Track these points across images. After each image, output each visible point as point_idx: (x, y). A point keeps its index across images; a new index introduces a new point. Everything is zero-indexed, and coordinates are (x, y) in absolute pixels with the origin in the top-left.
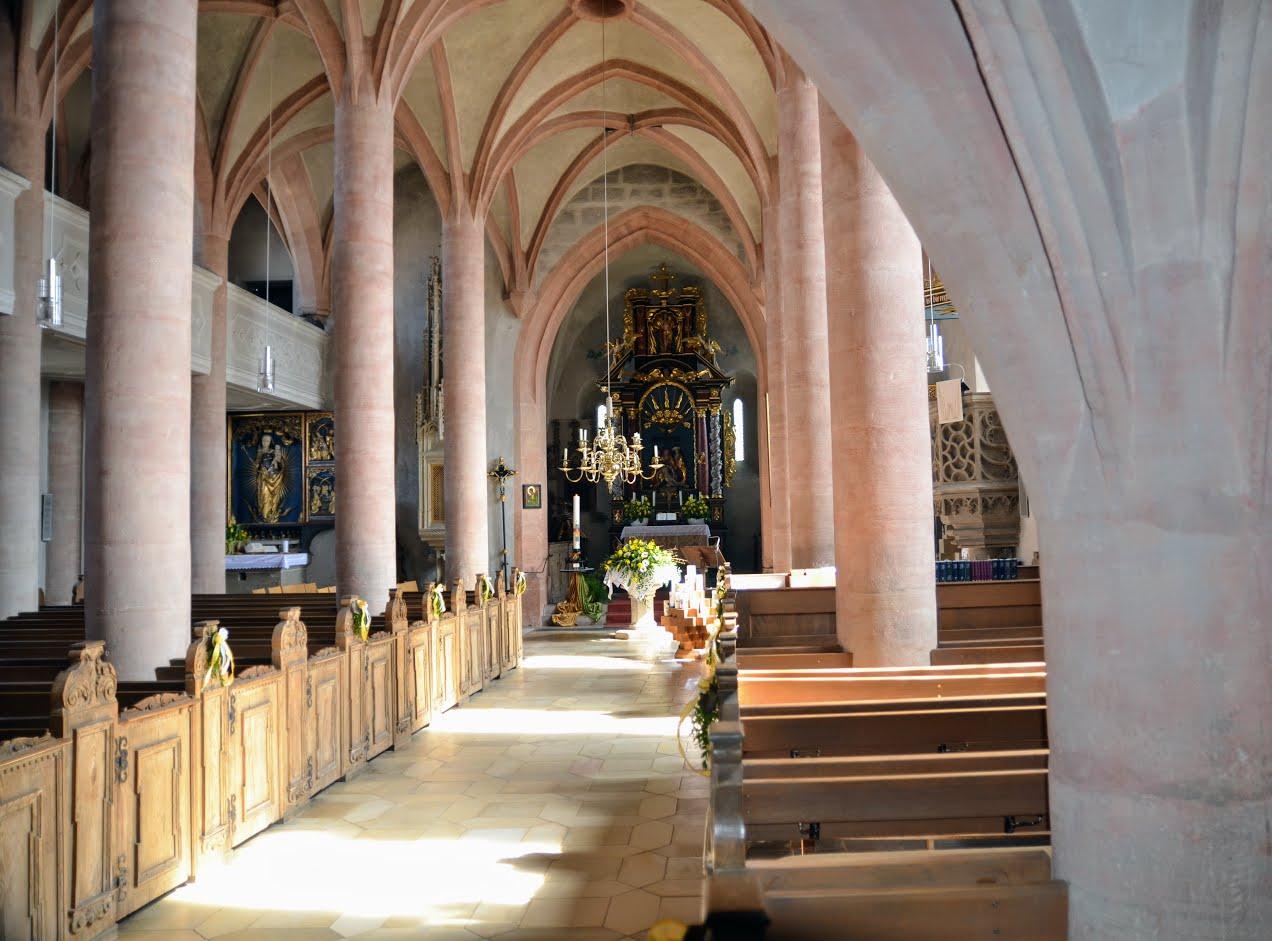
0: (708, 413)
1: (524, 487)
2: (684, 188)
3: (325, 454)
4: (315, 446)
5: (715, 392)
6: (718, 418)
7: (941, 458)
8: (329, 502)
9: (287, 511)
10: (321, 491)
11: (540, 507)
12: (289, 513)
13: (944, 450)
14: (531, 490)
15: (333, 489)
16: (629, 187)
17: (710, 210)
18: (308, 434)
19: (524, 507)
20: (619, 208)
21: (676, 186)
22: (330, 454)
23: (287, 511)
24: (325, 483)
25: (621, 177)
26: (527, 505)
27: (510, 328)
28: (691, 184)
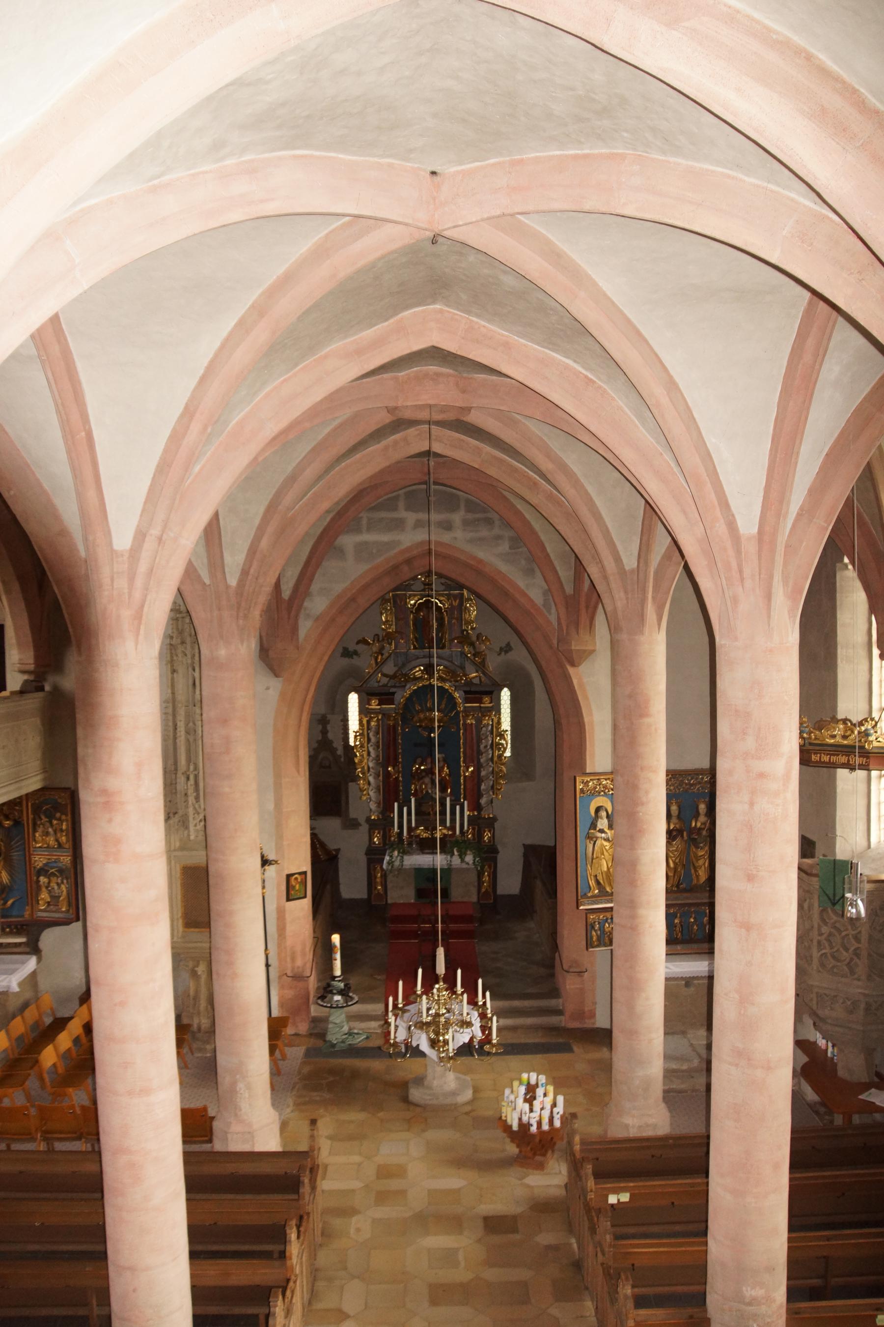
0: (479, 721)
1: (289, 876)
2: (478, 520)
3: (51, 840)
4: (40, 830)
5: (486, 699)
6: (490, 727)
7: (815, 943)
8: (60, 897)
9: (10, 902)
10: (49, 883)
11: (305, 897)
12: (13, 904)
13: (821, 934)
14: (296, 879)
15: (62, 882)
16: (411, 517)
17: (510, 548)
18: (31, 816)
19: (288, 899)
21: (470, 516)
22: (57, 840)
23: (10, 902)
24: (53, 874)
25: (401, 504)
26: (291, 898)
27: (268, 688)
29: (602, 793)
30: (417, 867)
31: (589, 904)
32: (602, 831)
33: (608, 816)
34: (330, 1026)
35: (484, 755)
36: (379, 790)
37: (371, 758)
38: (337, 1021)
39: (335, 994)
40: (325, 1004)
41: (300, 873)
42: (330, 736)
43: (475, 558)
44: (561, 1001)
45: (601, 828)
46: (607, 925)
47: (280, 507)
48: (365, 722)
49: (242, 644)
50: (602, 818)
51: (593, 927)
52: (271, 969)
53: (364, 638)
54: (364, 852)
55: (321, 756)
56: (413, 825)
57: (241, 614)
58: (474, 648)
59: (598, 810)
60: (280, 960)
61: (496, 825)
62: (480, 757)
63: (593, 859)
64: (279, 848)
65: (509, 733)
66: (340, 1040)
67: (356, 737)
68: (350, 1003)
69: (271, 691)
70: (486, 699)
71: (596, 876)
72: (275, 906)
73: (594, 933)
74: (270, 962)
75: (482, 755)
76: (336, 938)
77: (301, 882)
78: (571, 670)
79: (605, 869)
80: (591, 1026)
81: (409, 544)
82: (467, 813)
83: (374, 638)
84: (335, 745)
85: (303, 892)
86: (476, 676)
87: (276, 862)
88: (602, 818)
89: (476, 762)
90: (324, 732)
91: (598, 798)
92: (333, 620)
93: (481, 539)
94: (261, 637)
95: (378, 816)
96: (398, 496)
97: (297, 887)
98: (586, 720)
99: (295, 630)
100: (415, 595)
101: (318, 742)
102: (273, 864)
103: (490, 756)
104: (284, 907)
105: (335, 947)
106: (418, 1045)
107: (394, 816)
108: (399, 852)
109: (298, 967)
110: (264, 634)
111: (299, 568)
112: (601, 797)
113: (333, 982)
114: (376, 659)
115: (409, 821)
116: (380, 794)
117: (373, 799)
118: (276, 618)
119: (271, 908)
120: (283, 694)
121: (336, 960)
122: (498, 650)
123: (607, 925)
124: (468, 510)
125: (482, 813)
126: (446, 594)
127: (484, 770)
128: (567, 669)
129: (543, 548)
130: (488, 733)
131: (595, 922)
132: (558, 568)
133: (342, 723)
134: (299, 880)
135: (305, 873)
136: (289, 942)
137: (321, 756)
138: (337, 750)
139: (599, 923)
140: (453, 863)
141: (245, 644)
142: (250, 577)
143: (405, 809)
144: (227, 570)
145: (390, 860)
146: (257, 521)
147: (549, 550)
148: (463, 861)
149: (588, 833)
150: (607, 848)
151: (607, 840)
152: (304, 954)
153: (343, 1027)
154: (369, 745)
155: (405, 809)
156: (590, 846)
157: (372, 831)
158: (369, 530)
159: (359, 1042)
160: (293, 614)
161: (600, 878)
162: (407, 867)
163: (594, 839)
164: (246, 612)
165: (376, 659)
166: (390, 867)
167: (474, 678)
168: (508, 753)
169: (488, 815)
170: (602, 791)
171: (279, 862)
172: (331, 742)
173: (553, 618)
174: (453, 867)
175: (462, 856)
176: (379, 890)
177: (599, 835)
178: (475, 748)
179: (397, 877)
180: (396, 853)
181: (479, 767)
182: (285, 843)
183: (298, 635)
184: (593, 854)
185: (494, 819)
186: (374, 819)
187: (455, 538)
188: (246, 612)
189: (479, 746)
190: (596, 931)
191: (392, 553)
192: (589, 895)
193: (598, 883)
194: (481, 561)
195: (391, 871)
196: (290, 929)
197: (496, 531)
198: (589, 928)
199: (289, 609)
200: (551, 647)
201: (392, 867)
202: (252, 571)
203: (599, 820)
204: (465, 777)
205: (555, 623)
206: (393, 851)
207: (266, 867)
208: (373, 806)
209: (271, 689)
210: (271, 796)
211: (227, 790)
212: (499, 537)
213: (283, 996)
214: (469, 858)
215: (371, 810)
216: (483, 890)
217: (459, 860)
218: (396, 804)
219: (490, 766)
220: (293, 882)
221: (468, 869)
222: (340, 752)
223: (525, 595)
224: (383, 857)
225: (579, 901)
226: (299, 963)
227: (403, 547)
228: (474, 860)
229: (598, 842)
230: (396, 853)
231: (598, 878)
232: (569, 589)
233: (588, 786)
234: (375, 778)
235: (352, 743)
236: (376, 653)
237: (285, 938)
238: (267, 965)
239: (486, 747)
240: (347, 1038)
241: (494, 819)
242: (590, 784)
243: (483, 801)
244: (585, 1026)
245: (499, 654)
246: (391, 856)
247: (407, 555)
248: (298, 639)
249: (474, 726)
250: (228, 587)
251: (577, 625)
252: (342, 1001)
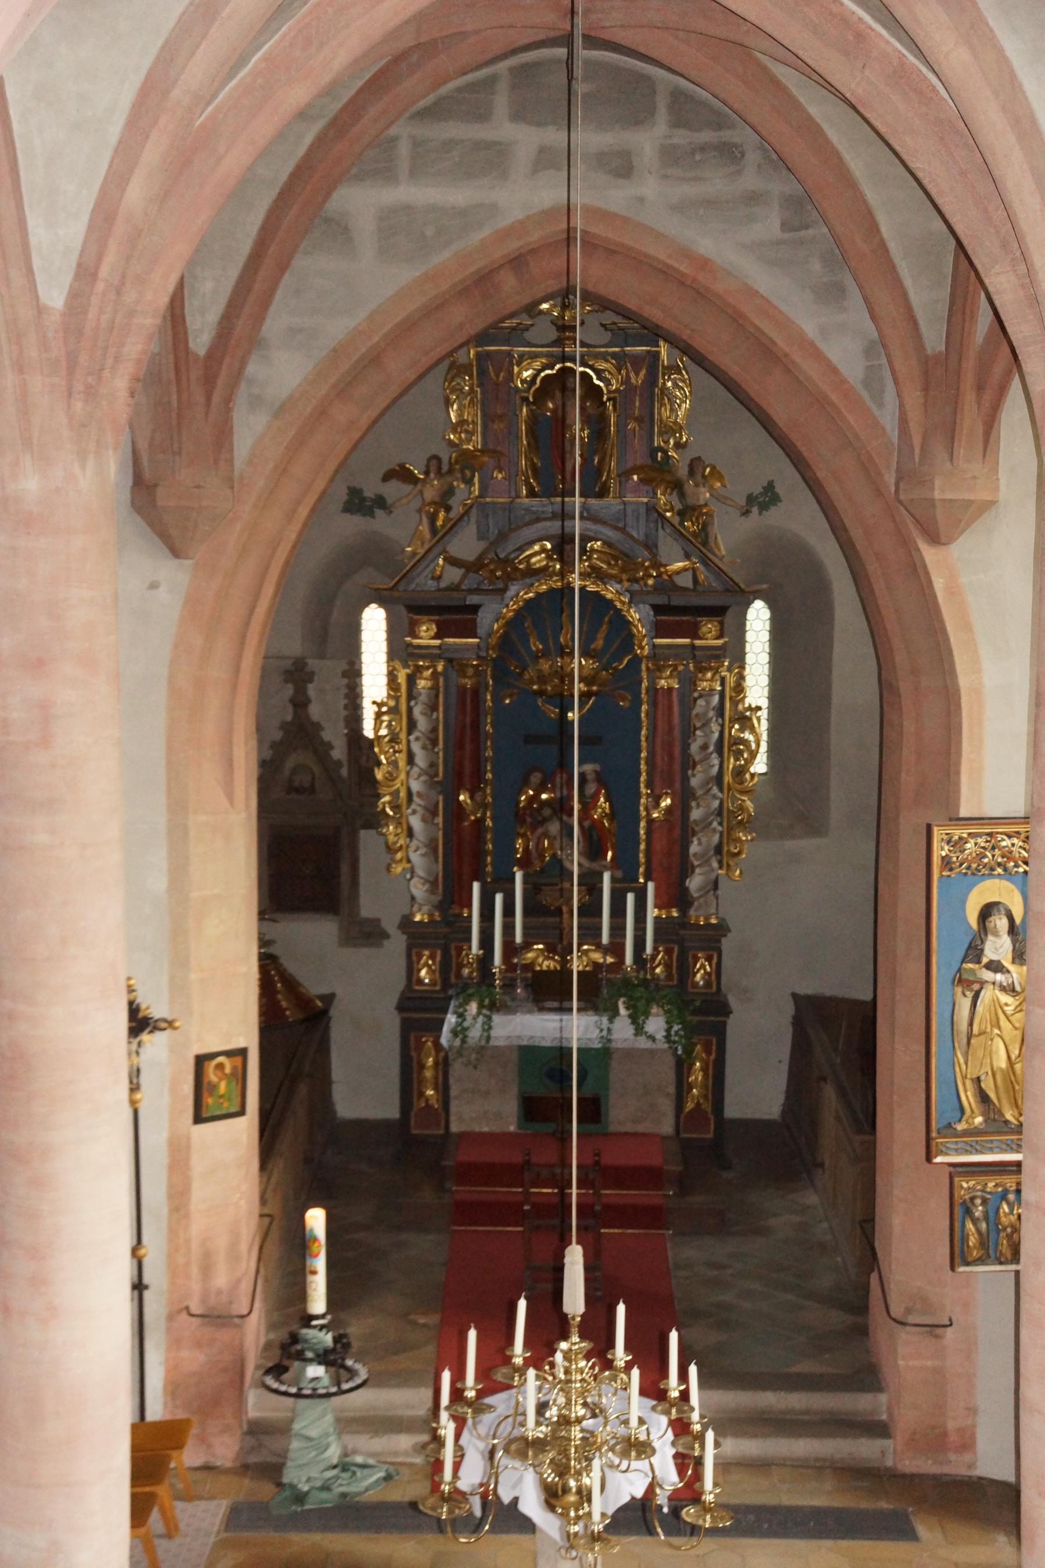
0: (689, 682)
1: (201, 1061)
5: (709, 627)
6: (716, 699)
11: (241, 1112)
14: (220, 1066)
17: (785, 226)
20: (493, 209)
21: (682, 137)
25: (501, 101)
26: (205, 1115)
27: (154, 586)
28: (727, 135)
29: (999, 870)
30: (525, 1043)
31: (958, 1152)
32: (995, 966)
33: (1012, 930)
34: (295, 1444)
35: (699, 768)
36: (435, 851)
37: (415, 770)
38: (313, 1433)
39: (310, 1361)
40: (283, 1388)
41: (229, 1054)
42: (315, 711)
43: (686, 254)
44: (883, 1398)
45: (995, 957)
46: (1005, 1208)
47: (176, 93)
48: (402, 679)
49: (83, 467)
50: (996, 934)
51: (968, 1212)
52: (147, 1294)
53: (402, 466)
54: (394, 1005)
55: (290, 763)
56: (519, 939)
57: (79, 387)
58: (682, 495)
59: (987, 911)
60: (174, 1271)
61: (726, 944)
62: (690, 772)
63: (970, 1036)
64: (178, 988)
65: (764, 714)
66: (319, 1484)
67: (379, 715)
68: (345, 1386)
69: (162, 594)
70: (709, 627)
71: (978, 1080)
72: (165, 1135)
73: (970, 1226)
74: (147, 1279)
75: (694, 767)
76: (316, 1219)
77: (234, 1073)
78: (929, 554)
79: (1002, 1063)
80: (963, 1471)
81: (520, 215)
82: (652, 912)
83: (428, 466)
84: (327, 735)
85: (237, 1100)
86: (685, 569)
87: (171, 1024)
88: (996, 934)
89: (678, 785)
90: (300, 703)
91: (989, 883)
92: (322, 413)
93: (709, 203)
94: (135, 454)
95: (431, 915)
96: (494, 79)
97: (223, 1087)
98: (964, 681)
99: (223, 435)
100: (534, 356)
101: (284, 726)
102: (164, 1029)
103: (716, 769)
104: (188, 1138)
105: (316, 1239)
106: (516, 1500)
107: (470, 916)
108: (481, 1006)
109: (219, 1292)
110: (143, 445)
111: (234, 272)
112: (997, 881)
113: (304, 1331)
114: (433, 519)
115: (509, 928)
116: (436, 860)
117: (420, 872)
118: (175, 404)
119: (155, 1139)
120: (192, 602)
121: (314, 1273)
122: (743, 502)
123: (1005, 1208)
124: (678, 121)
125: (692, 912)
126: (614, 355)
127: (698, 806)
128: (918, 550)
129: (873, 228)
130: (711, 714)
131: (972, 1199)
132: (908, 283)
133: (345, 681)
134: (228, 1070)
135: (243, 1052)
136: (196, 1228)
137: (290, 763)
138: (332, 747)
139: (985, 1202)
140: (615, 1036)
141: (91, 463)
142: (100, 286)
143: (499, 898)
144: (37, 263)
145: (459, 1024)
146: (114, 130)
147: (885, 231)
148: (639, 1030)
149: (959, 970)
150: (1009, 1010)
151: (1010, 989)
152: (234, 1257)
153: (327, 1447)
154: (412, 738)
155: (499, 898)
156: (964, 1004)
157: (414, 951)
158: (414, 173)
159: (367, 1489)
160: (216, 398)
161: (988, 1086)
162: (501, 1043)
163: (976, 987)
164: (90, 379)
165: (433, 519)
166: (457, 1043)
167: (678, 572)
168: (760, 766)
169: (707, 918)
170: (999, 865)
171: (177, 1024)
172: (318, 727)
173: (889, 420)
174: (614, 1045)
175: (637, 1020)
176: (427, 1100)
177: (988, 975)
178: (677, 751)
179: (475, 1067)
180: (473, 1007)
181: (685, 798)
182: (193, 976)
183: (231, 450)
184: (971, 1024)
185: (722, 929)
186: (421, 922)
187: (641, 200)
188: (90, 379)
189: (686, 746)
190: (975, 1221)
191: (477, 237)
192: (960, 1127)
193: (983, 1097)
194: (705, 264)
195: (460, 1053)
196: (201, 1195)
197: (750, 180)
198: (958, 1211)
199: (209, 381)
200: (879, 492)
201: (464, 1041)
202: (104, 271)
203: (990, 938)
204: (650, 821)
205: (894, 435)
206: (467, 1002)
207: (145, 1037)
208: (418, 889)
209: (163, 588)
210: (159, 857)
211: (43, 838)
212: (753, 198)
214: (656, 1024)
215: (413, 898)
216: (690, 1106)
217: (630, 1030)
218: (476, 886)
219: (715, 797)
220: (211, 1074)
221: (652, 1052)
222: (339, 752)
223: (818, 355)
224: (441, 1016)
225: (933, 1143)
226: (221, 1280)
227: (504, 222)
228: (668, 1030)
229: (987, 995)
230: (473, 1007)
231: (983, 1085)
232: (934, 339)
233: (963, 851)
234: (424, 820)
235: (368, 732)
236: (433, 503)
237: (187, 1215)
238: (139, 1287)
239: (704, 747)
240: (336, 1477)
241: (722, 929)
242: (968, 846)
243: (694, 883)
244: (946, 1469)
245: (746, 513)
246: (461, 1016)
247: (513, 246)
248: (231, 461)
249: (675, 694)
250: (40, 310)
251: (950, 433)
252: (326, 1381)
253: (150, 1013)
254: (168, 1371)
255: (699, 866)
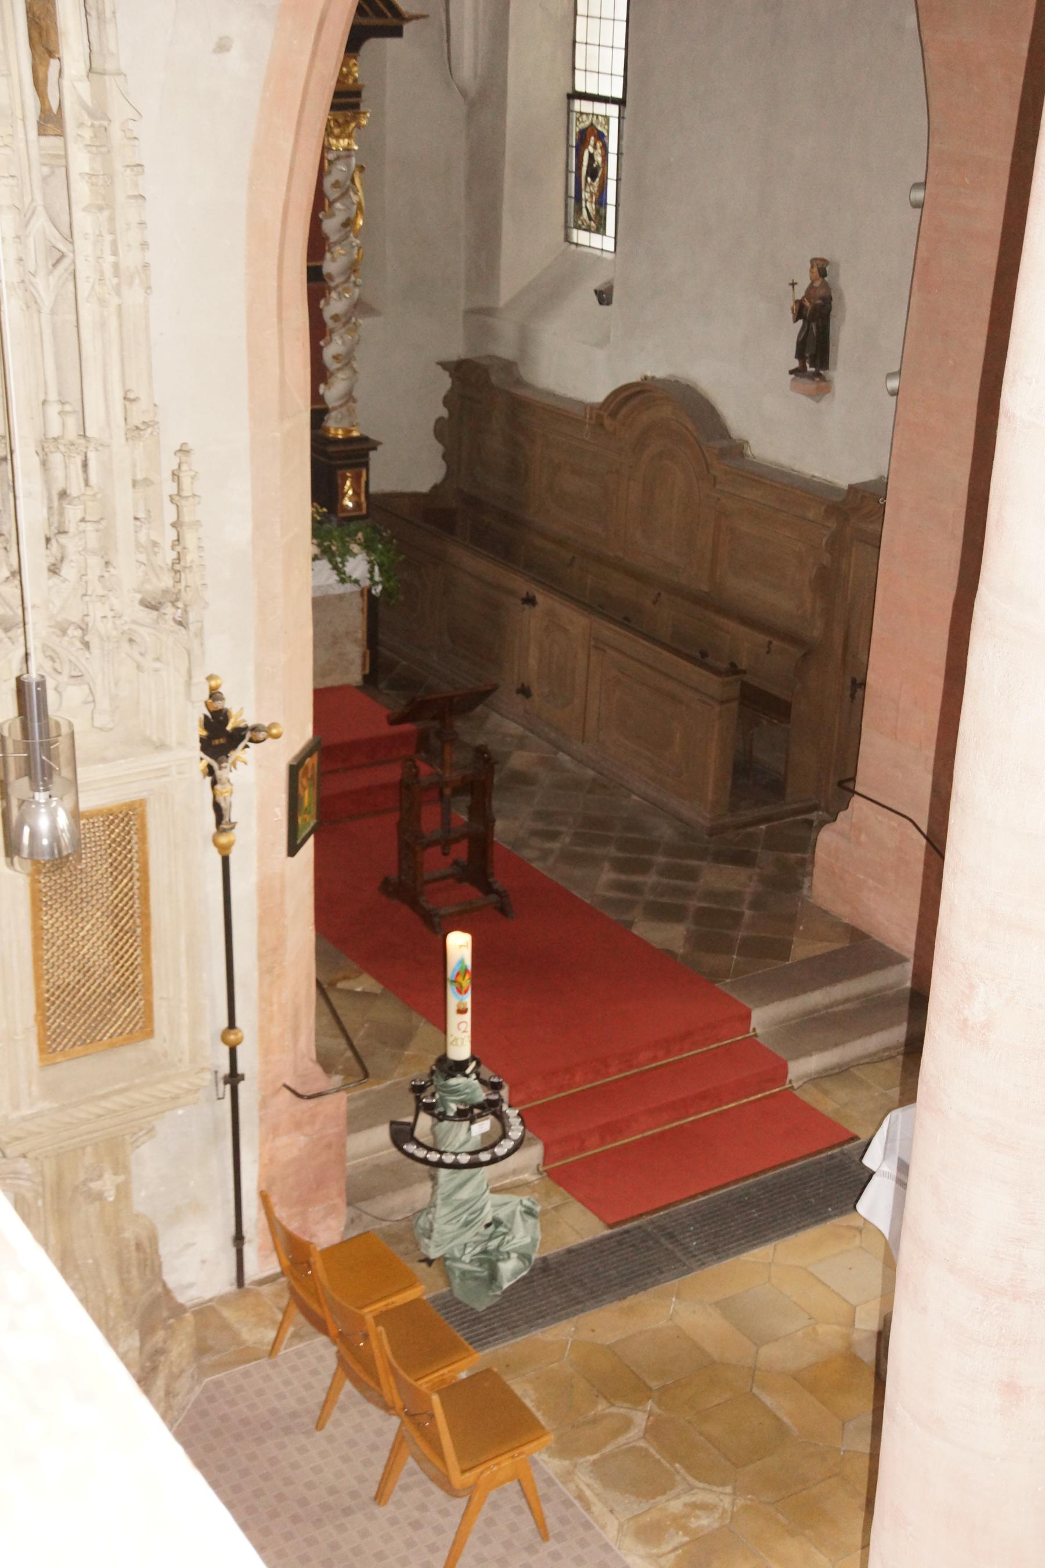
27: (222, 46)
52: (242, 1086)
72: (253, 879)
74: (241, 1069)
213: (272, 1160)
253: (244, 721)
254: (263, 1166)
255: (339, 370)
